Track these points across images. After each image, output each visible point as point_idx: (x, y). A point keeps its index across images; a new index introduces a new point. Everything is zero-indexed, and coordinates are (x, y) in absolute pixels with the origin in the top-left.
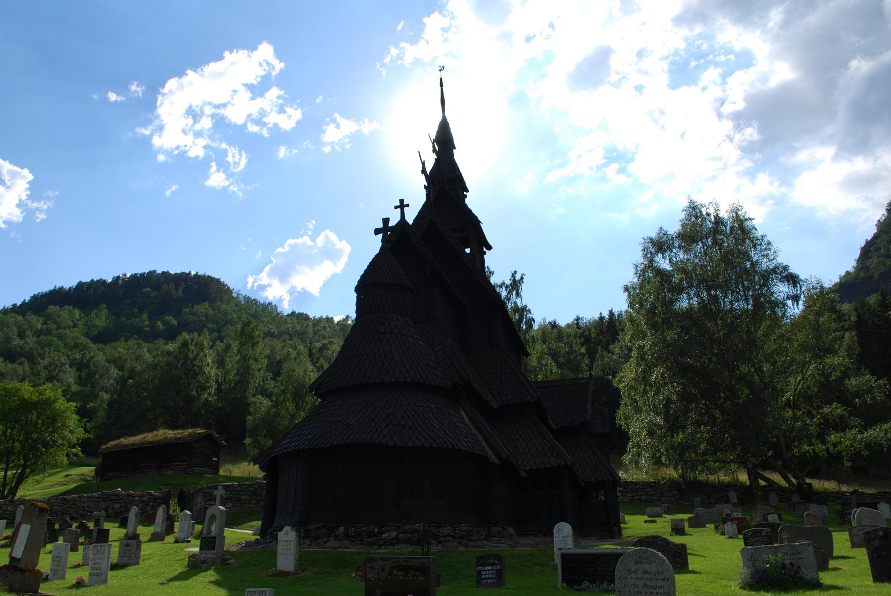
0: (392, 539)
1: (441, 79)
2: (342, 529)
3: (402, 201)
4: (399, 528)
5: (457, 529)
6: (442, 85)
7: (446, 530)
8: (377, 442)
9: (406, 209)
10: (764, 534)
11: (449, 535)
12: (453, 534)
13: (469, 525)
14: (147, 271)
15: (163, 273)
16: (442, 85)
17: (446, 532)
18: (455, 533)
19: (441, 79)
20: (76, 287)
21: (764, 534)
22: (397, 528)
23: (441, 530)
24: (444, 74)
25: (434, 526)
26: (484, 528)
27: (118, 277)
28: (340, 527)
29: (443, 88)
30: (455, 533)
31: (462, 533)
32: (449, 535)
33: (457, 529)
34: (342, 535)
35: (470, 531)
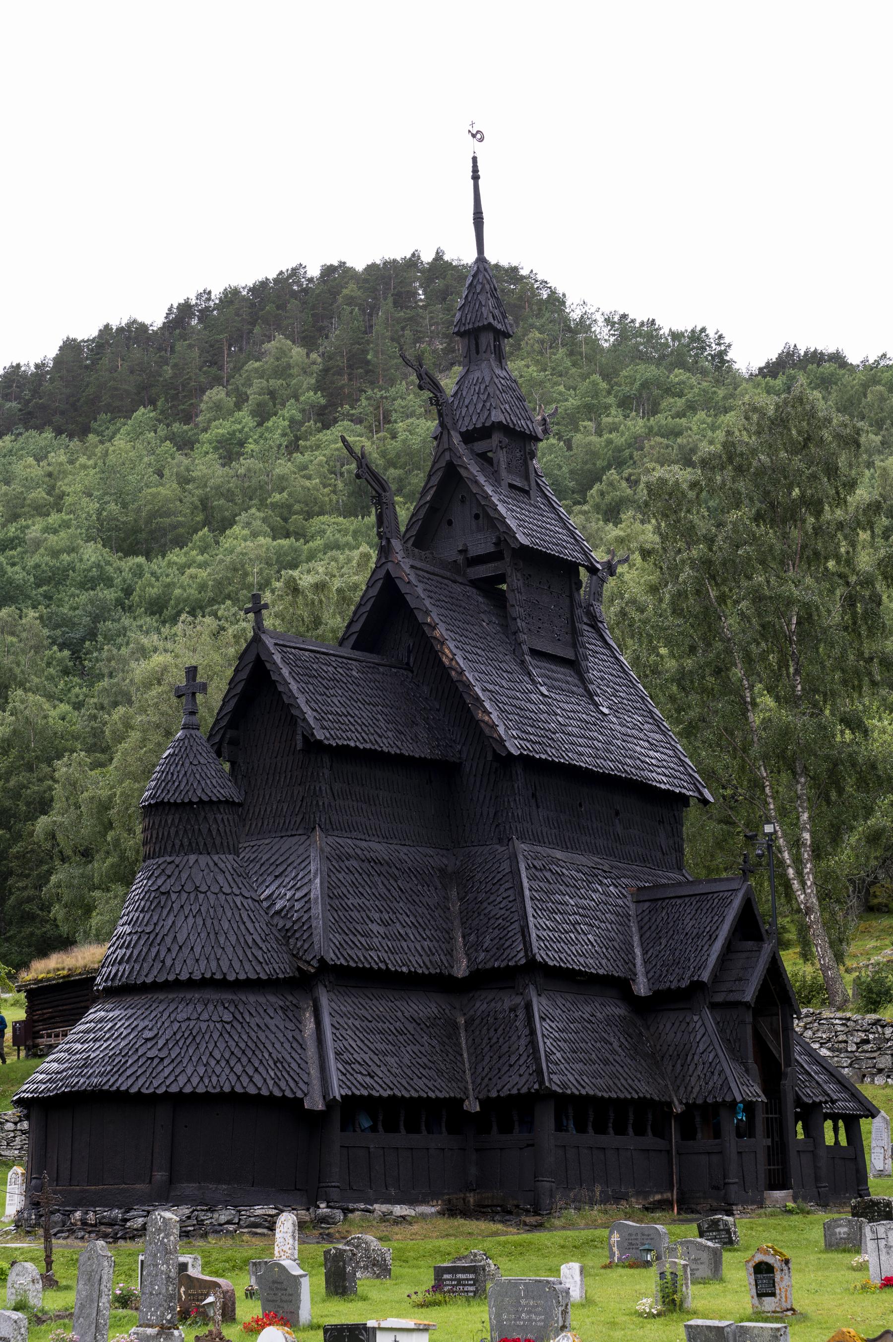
0: (136, 1230)
1: (475, 159)
2: (78, 1214)
4: (148, 1212)
5: (243, 1213)
6: (476, 177)
7: (223, 1216)
8: (114, 1088)
9: (263, 611)
10: (721, 1227)
11: (229, 1222)
12: (236, 1220)
14: (272, 275)
15: (328, 271)
16: (476, 177)
17: (223, 1218)
18: (240, 1219)
19: (475, 159)
20: (57, 360)
21: (721, 1227)
22: (145, 1213)
23: (216, 1215)
25: (203, 1210)
26: (308, 1210)
27: (185, 309)
28: (76, 1211)
29: (480, 182)
31: (252, 1219)
32: (229, 1222)
33: (243, 1213)
34: (79, 1223)
35: (269, 1215)
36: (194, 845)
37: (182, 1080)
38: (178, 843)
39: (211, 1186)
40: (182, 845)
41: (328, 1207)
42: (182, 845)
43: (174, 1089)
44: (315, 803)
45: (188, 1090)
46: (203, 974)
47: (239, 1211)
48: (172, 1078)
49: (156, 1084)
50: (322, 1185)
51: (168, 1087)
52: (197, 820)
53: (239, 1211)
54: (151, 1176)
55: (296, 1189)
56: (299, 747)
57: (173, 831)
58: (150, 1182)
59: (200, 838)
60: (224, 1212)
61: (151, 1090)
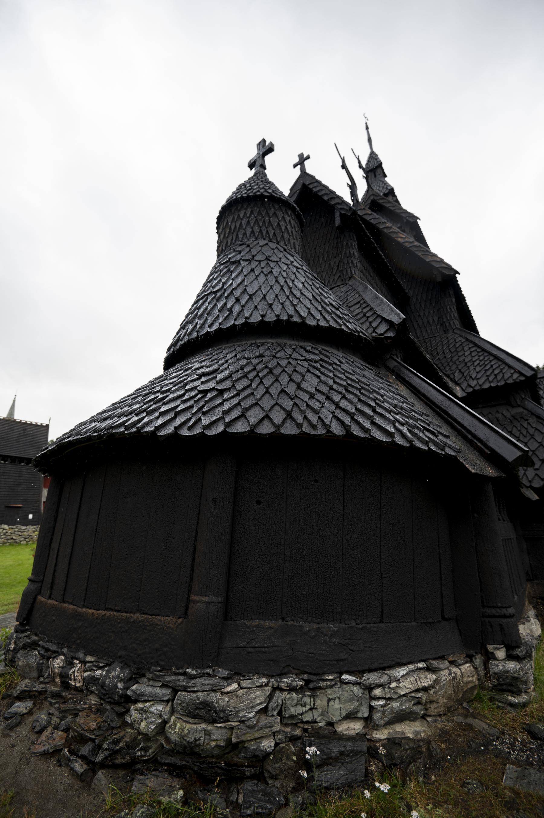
2: (58, 662)
3: (301, 156)
5: (377, 692)
6: (367, 128)
13: (420, 665)
16: (367, 128)
18: (371, 708)
23: (321, 702)
24: (366, 116)
29: (369, 130)
30: (371, 708)
31: (395, 705)
33: (377, 692)
36: (264, 233)
37: (254, 416)
38: (249, 230)
39: (307, 627)
40: (253, 232)
41: (510, 657)
42: (253, 232)
43: (240, 428)
44: (350, 261)
45: (266, 429)
46: (278, 316)
47: (370, 688)
48: (237, 413)
49: (205, 421)
50: (489, 611)
51: (229, 424)
52: (267, 213)
53: (370, 688)
54: (188, 601)
55: (444, 619)
56: (338, 222)
57: (244, 222)
58: (186, 614)
59: (271, 229)
60: (337, 691)
61: (198, 430)
